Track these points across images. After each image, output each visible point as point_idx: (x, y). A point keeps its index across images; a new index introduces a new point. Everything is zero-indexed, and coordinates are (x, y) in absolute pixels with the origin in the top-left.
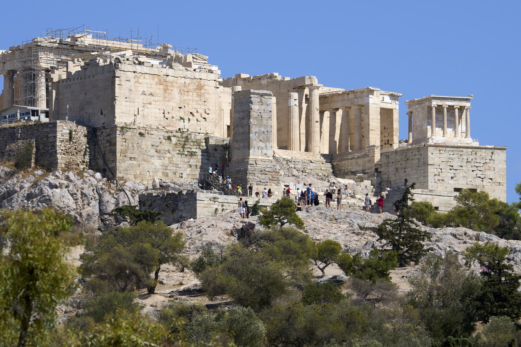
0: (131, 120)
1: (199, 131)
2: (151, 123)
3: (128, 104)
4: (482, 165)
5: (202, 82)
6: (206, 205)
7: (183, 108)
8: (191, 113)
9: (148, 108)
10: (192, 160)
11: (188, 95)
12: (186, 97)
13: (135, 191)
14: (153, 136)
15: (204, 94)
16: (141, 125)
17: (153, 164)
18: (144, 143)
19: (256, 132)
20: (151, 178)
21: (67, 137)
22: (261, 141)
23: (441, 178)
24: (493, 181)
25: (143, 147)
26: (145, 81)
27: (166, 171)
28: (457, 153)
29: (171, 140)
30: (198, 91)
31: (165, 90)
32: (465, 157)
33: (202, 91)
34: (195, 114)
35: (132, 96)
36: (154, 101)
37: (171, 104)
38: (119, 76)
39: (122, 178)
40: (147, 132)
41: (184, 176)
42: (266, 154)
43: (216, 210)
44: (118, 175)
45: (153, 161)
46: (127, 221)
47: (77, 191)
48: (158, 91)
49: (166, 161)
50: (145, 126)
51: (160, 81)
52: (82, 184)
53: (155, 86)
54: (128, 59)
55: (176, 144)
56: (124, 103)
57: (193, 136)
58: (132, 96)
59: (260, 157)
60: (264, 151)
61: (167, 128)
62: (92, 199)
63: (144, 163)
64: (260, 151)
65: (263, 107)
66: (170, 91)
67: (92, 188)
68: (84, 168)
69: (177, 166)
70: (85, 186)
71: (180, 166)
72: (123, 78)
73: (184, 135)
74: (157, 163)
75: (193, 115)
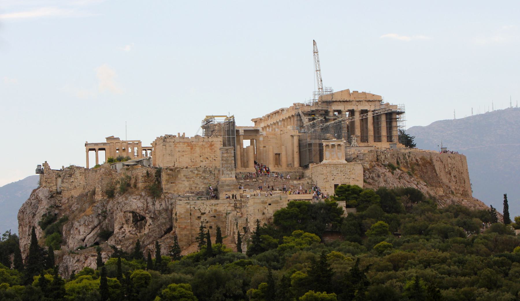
31: (192, 149)
33: (213, 147)
39: (167, 193)
48: (187, 150)
49: (192, 182)
51: (188, 145)
74: (186, 184)
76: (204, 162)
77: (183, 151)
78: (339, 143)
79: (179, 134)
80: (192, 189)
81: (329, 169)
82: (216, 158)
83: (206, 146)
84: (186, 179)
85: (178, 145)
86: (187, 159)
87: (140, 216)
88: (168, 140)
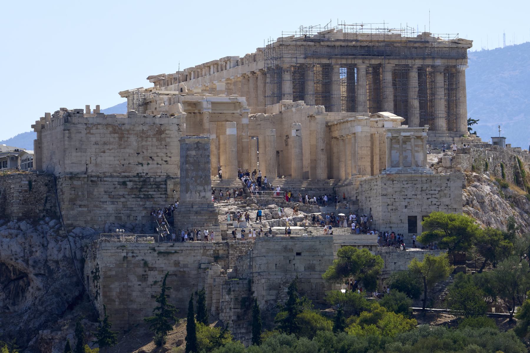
0: (83, 169)
1: (159, 174)
2: (105, 170)
4: (437, 192)
5: (162, 128)
6: (113, 254)
7: (141, 153)
9: (101, 157)
10: (148, 203)
11: (146, 141)
12: (144, 143)
13: (79, 237)
14: (106, 183)
15: (165, 138)
16: (93, 174)
17: (105, 209)
18: (96, 190)
20: (103, 223)
21: (26, 188)
23: (394, 208)
24: (449, 207)
25: (95, 193)
26: (98, 131)
27: (119, 215)
28: (410, 182)
29: (126, 185)
31: (121, 138)
32: (419, 186)
33: (163, 136)
34: (155, 158)
35: (83, 147)
36: (108, 149)
37: (127, 150)
38: (69, 128)
39: (71, 225)
40: (99, 179)
41: (139, 218)
42: (204, 197)
43: (125, 258)
44: (66, 222)
45: (105, 206)
46: (65, 266)
47: (26, 239)
48: (112, 140)
49: (120, 206)
50: (98, 173)
51: (114, 130)
52: (32, 232)
53: (109, 135)
54: (78, 113)
55: (132, 188)
56: (74, 154)
57: (152, 179)
58: (83, 147)
60: (203, 194)
61: (123, 174)
62: (39, 246)
63: (95, 208)
64: (198, 194)
65: (200, 152)
66: (126, 139)
67: (42, 235)
68: (44, 216)
69: (131, 209)
70: (34, 235)
71: (134, 209)
72: (73, 130)
73: (142, 179)
74: (110, 208)
75: (153, 160)
76: (145, 167)
77: (105, 144)
78: (419, 134)
79: (88, 107)
80: (120, 218)
81: (397, 186)
82: (168, 159)
83: (150, 133)
84: (109, 199)
85: (93, 131)
86: (112, 158)
87: (14, 269)
88: (75, 120)
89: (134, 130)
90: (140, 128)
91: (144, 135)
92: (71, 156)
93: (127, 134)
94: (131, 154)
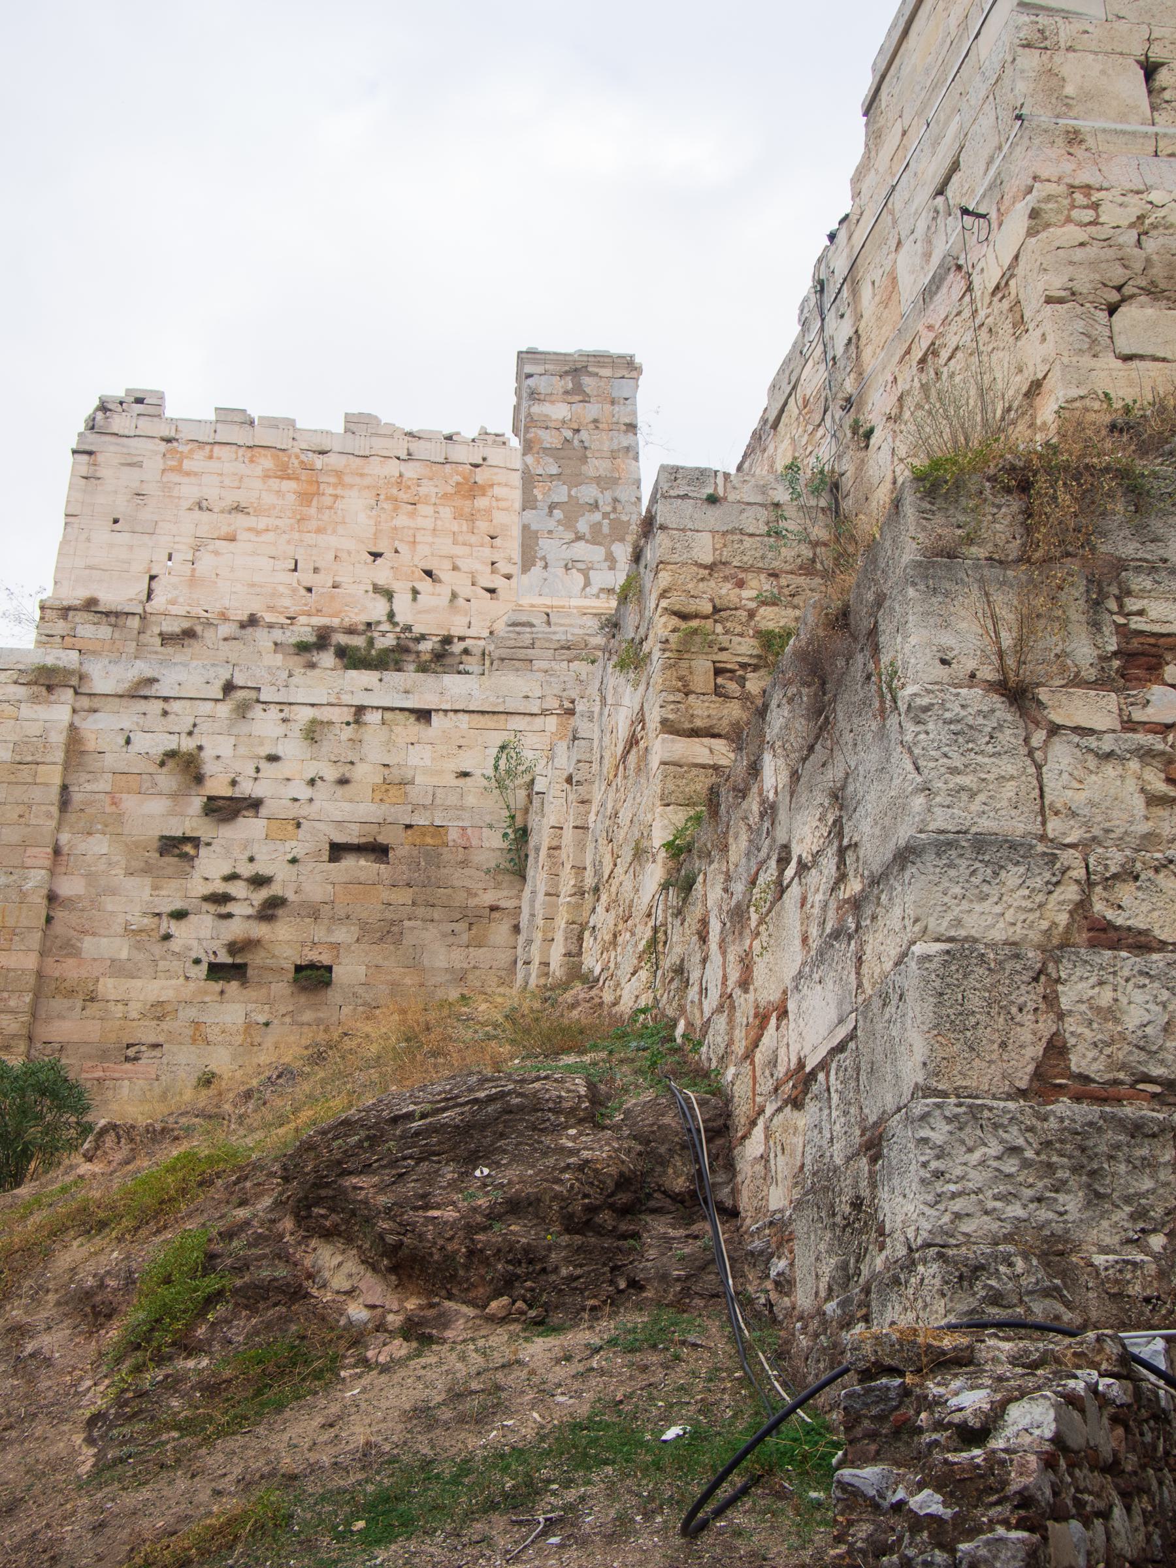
3: (125, 538)
8: (429, 573)
9: (216, 553)
11: (412, 515)
12: (402, 520)
19: (552, 507)
22: (579, 538)
26: (213, 465)
30: (459, 502)
31: (306, 498)
33: (482, 502)
36: (250, 529)
37: (331, 541)
48: (269, 499)
51: (284, 467)
59: (574, 602)
65: (592, 410)
66: (328, 501)
77: (238, 509)
82: (498, 582)
89: (362, 475)
90: (393, 468)
91: (403, 496)
92: (88, 540)
93: (335, 486)
94: (344, 555)
